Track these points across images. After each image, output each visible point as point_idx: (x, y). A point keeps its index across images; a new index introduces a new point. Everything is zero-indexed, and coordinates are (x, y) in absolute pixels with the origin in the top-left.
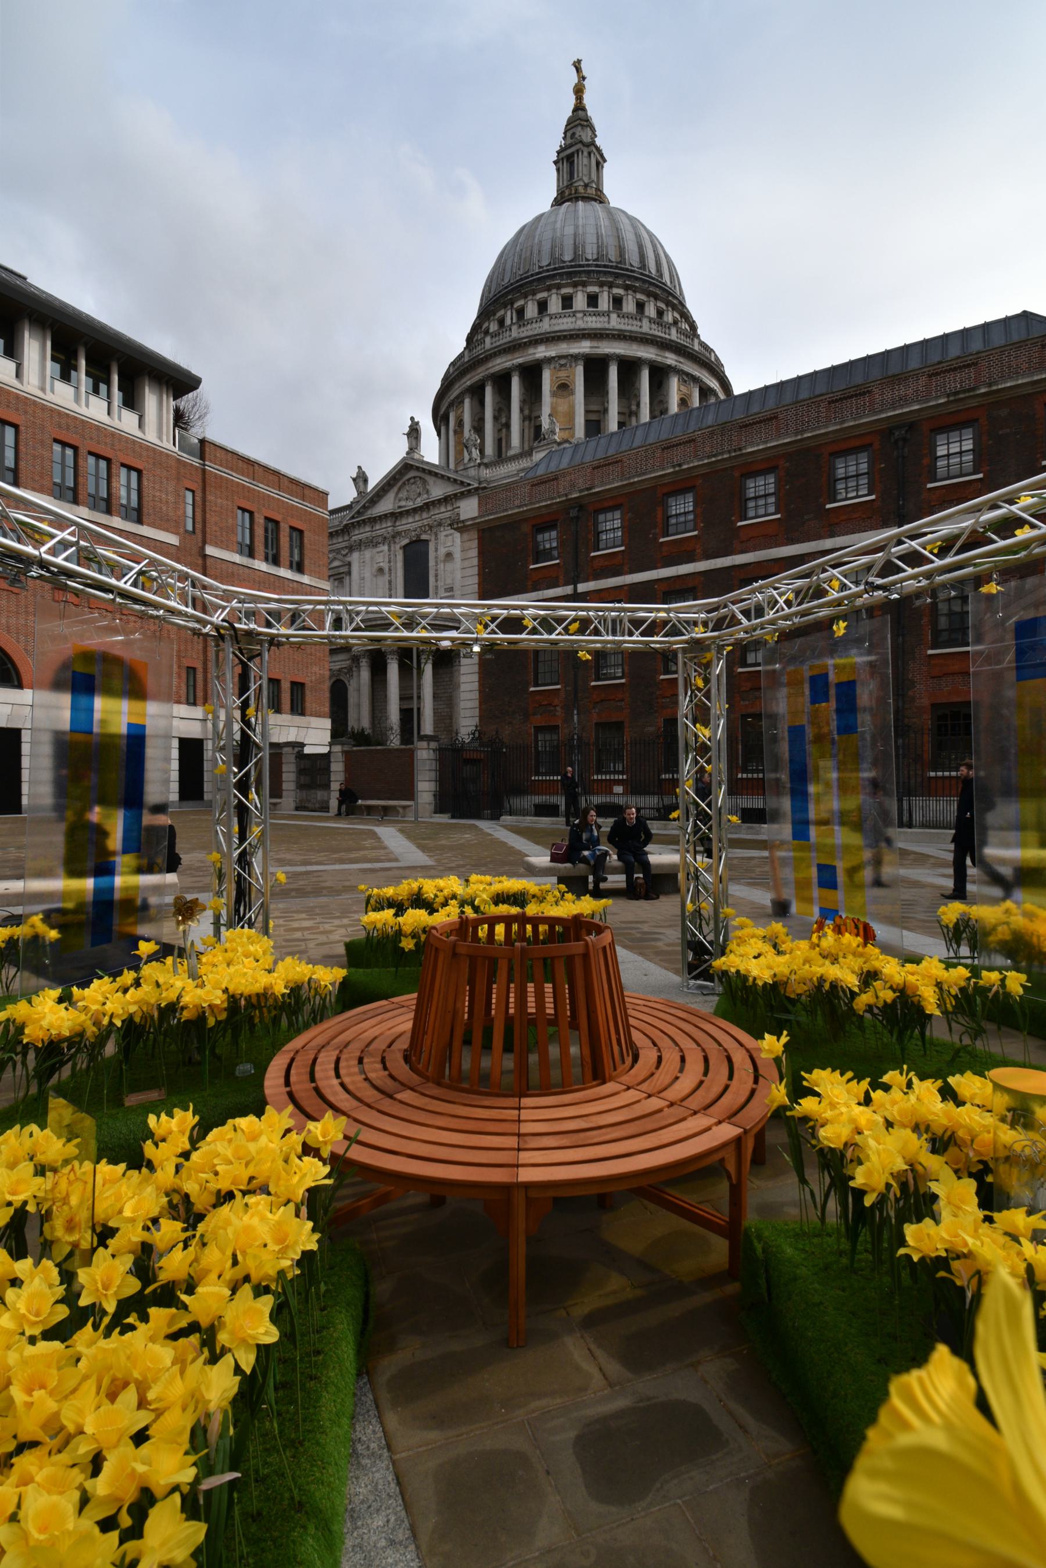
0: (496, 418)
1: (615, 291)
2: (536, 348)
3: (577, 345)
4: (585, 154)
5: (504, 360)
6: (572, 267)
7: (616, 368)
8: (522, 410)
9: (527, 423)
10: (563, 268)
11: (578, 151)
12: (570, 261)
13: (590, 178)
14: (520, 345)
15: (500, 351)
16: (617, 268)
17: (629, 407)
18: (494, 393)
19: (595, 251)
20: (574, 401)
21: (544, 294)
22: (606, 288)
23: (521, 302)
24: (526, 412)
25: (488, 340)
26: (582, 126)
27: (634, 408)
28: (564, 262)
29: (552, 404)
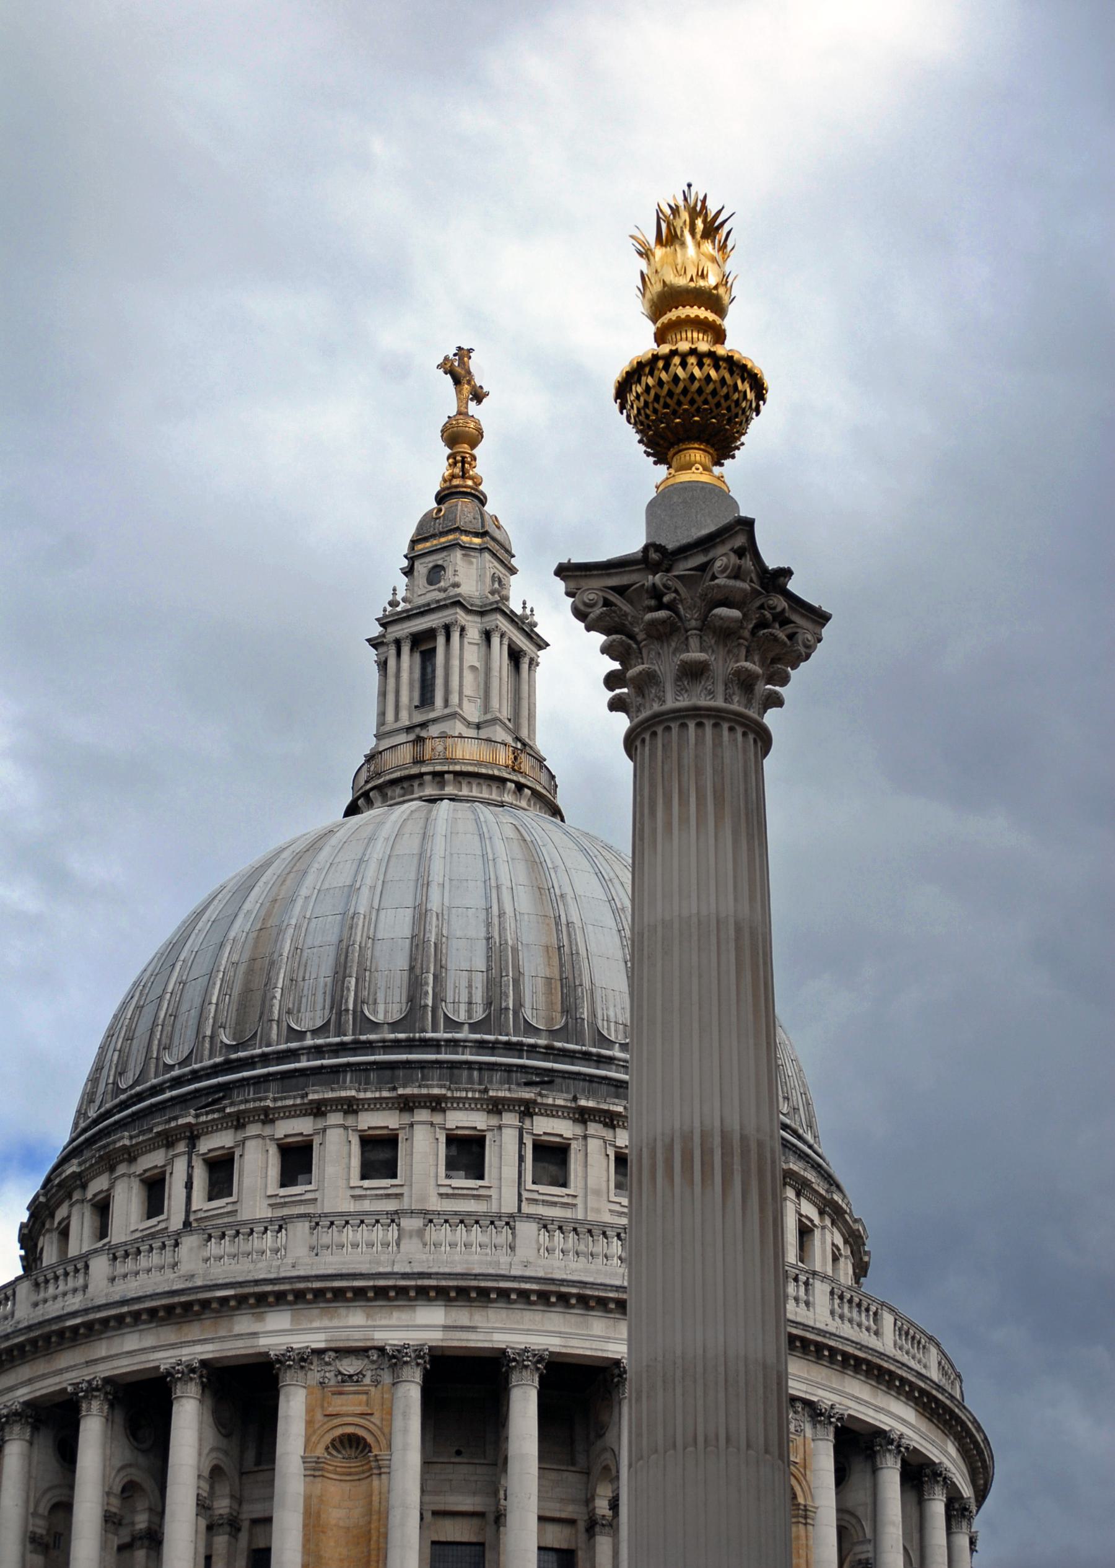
0: (111, 1521)
1: (544, 1126)
2: (260, 1317)
3: (399, 1317)
4: (474, 633)
5: (149, 1341)
6: (396, 1046)
7: (533, 1395)
8: (203, 1506)
9: (221, 1541)
10: (369, 1047)
11: (447, 629)
12: (394, 1026)
13: (486, 708)
14: (205, 1304)
15: (136, 1316)
16: (550, 1052)
17: (589, 1501)
18: (108, 1438)
19: (478, 997)
20: (385, 1496)
21: (303, 1126)
22: (510, 1119)
23: (222, 1140)
24: (222, 1506)
25: (100, 1266)
26: (463, 548)
27: (602, 1506)
28: (375, 1026)
29: (308, 1498)
